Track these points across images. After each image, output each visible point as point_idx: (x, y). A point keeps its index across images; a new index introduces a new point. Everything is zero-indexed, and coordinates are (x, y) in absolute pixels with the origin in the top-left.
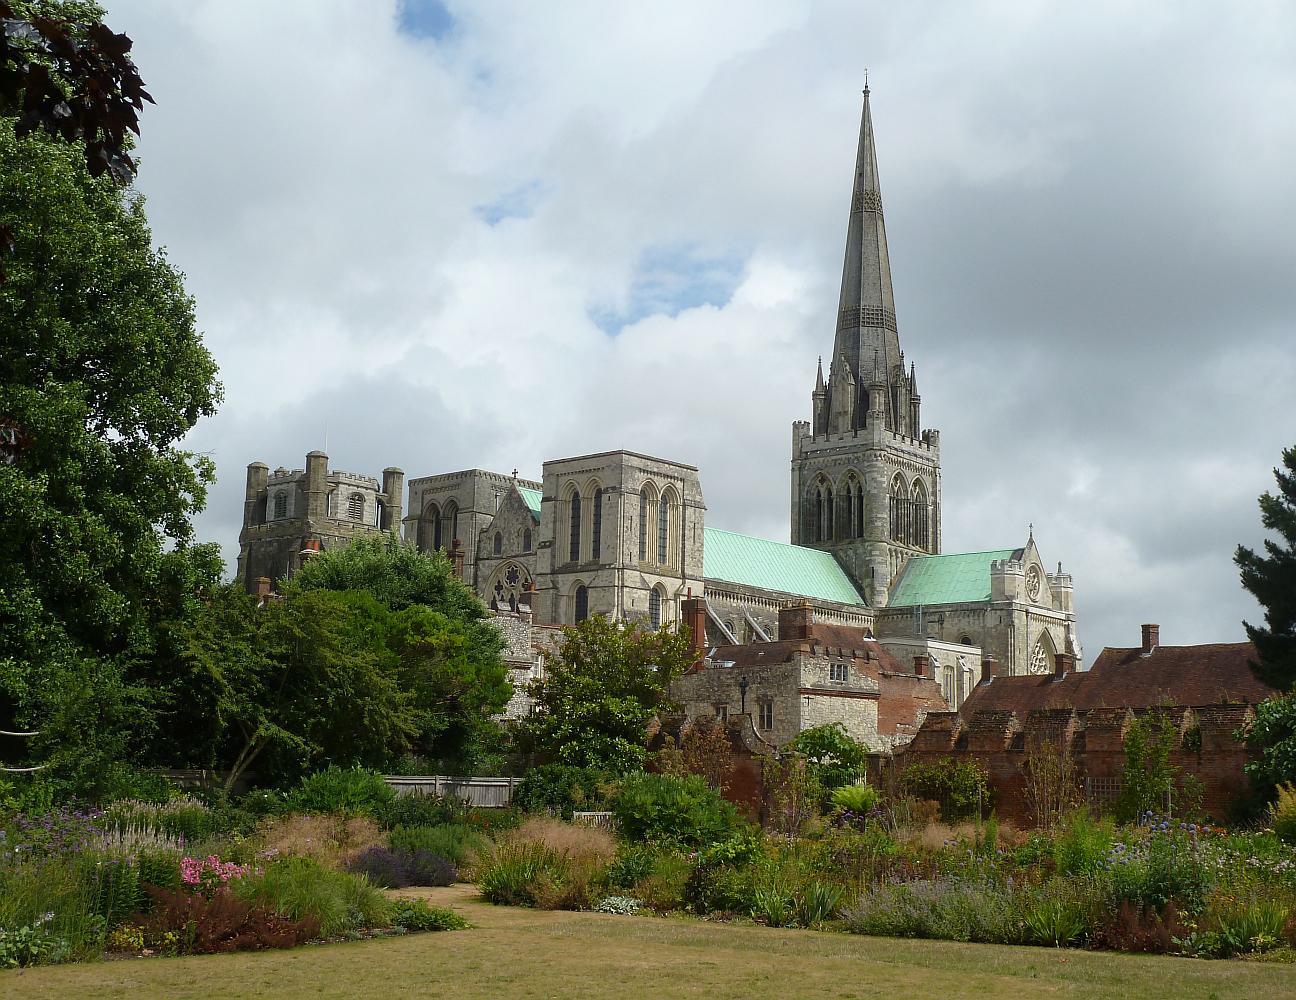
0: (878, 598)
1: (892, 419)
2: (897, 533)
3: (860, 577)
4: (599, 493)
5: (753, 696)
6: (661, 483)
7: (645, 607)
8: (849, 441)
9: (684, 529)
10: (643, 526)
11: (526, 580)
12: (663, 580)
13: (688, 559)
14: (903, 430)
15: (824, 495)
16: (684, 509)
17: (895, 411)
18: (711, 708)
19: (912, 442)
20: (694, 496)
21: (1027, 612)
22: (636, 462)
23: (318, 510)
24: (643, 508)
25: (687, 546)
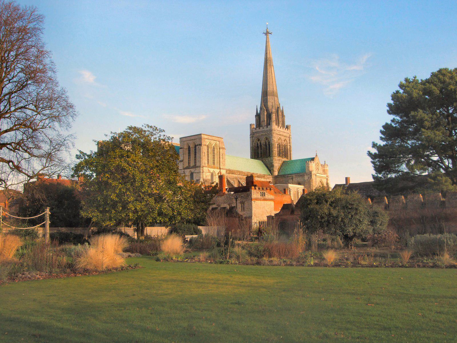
1: (278, 122)
3: (270, 167)
4: (195, 146)
5: (239, 201)
7: (209, 178)
8: (265, 129)
9: (220, 155)
10: (208, 155)
13: (221, 164)
14: (280, 125)
15: (259, 145)
18: (228, 205)
21: (316, 175)
22: (206, 137)
24: (208, 150)
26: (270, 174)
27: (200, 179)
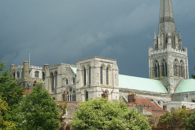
0: (171, 91)
1: (174, 45)
3: (167, 86)
6: (106, 64)
8: (162, 51)
12: (108, 89)
14: (177, 48)
15: (157, 65)
17: (175, 43)
24: (101, 71)
25: (114, 80)
26: (167, 92)
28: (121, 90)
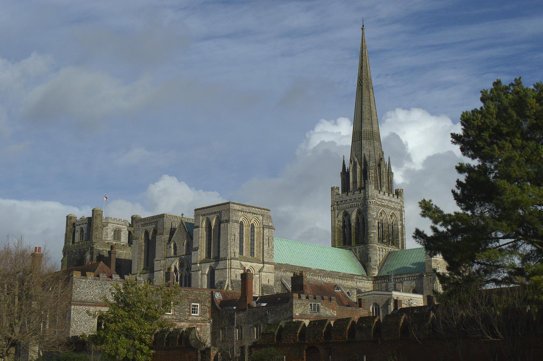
1: (379, 185)
2: (383, 240)
9: (263, 240)
11: (188, 266)
13: (265, 254)
14: (384, 189)
16: (263, 230)
19: (389, 195)
20: (269, 224)
22: (237, 207)
23: (98, 235)
25: (265, 248)
26: (365, 274)
27: (225, 281)
28: (278, 267)
